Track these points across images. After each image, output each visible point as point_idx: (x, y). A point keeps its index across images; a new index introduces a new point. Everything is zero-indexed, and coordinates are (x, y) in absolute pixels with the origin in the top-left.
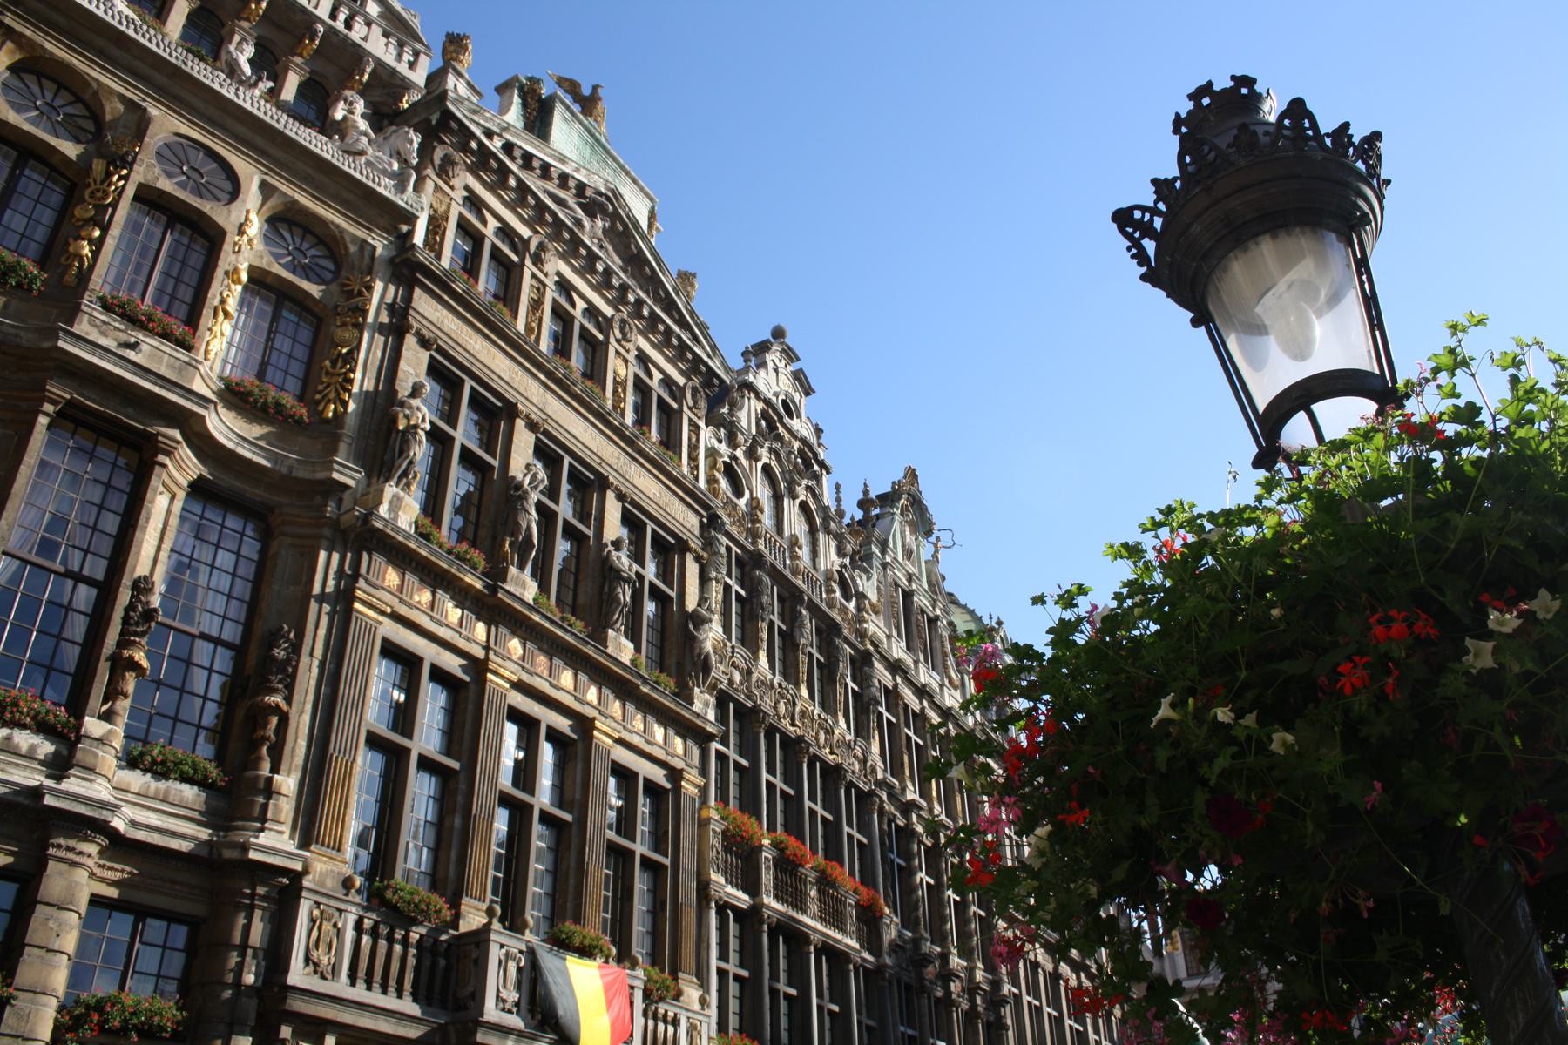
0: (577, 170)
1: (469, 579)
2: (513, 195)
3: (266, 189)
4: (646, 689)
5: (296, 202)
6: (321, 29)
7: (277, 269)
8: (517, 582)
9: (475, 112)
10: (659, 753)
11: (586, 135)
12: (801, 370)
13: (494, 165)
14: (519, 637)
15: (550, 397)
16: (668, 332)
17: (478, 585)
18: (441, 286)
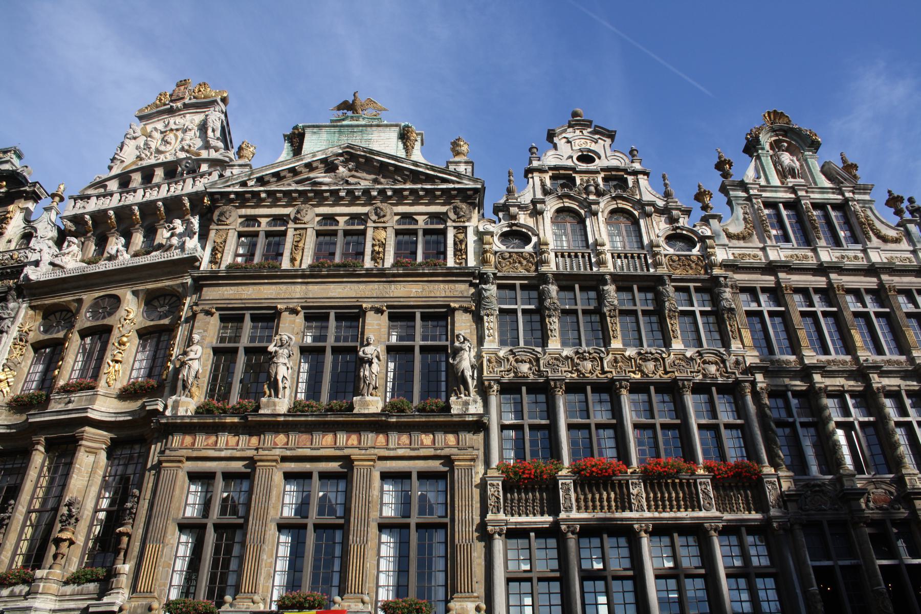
0: (314, 156)
1: (228, 420)
2: (270, 200)
3: (135, 293)
4: (394, 420)
5: (148, 289)
6: (160, 203)
7: (152, 323)
8: (267, 405)
9: (227, 181)
10: (431, 452)
11: (333, 130)
12: (596, 126)
13: (249, 196)
14: (282, 432)
15: (311, 287)
16: (413, 192)
17: (236, 420)
18: (213, 279)
